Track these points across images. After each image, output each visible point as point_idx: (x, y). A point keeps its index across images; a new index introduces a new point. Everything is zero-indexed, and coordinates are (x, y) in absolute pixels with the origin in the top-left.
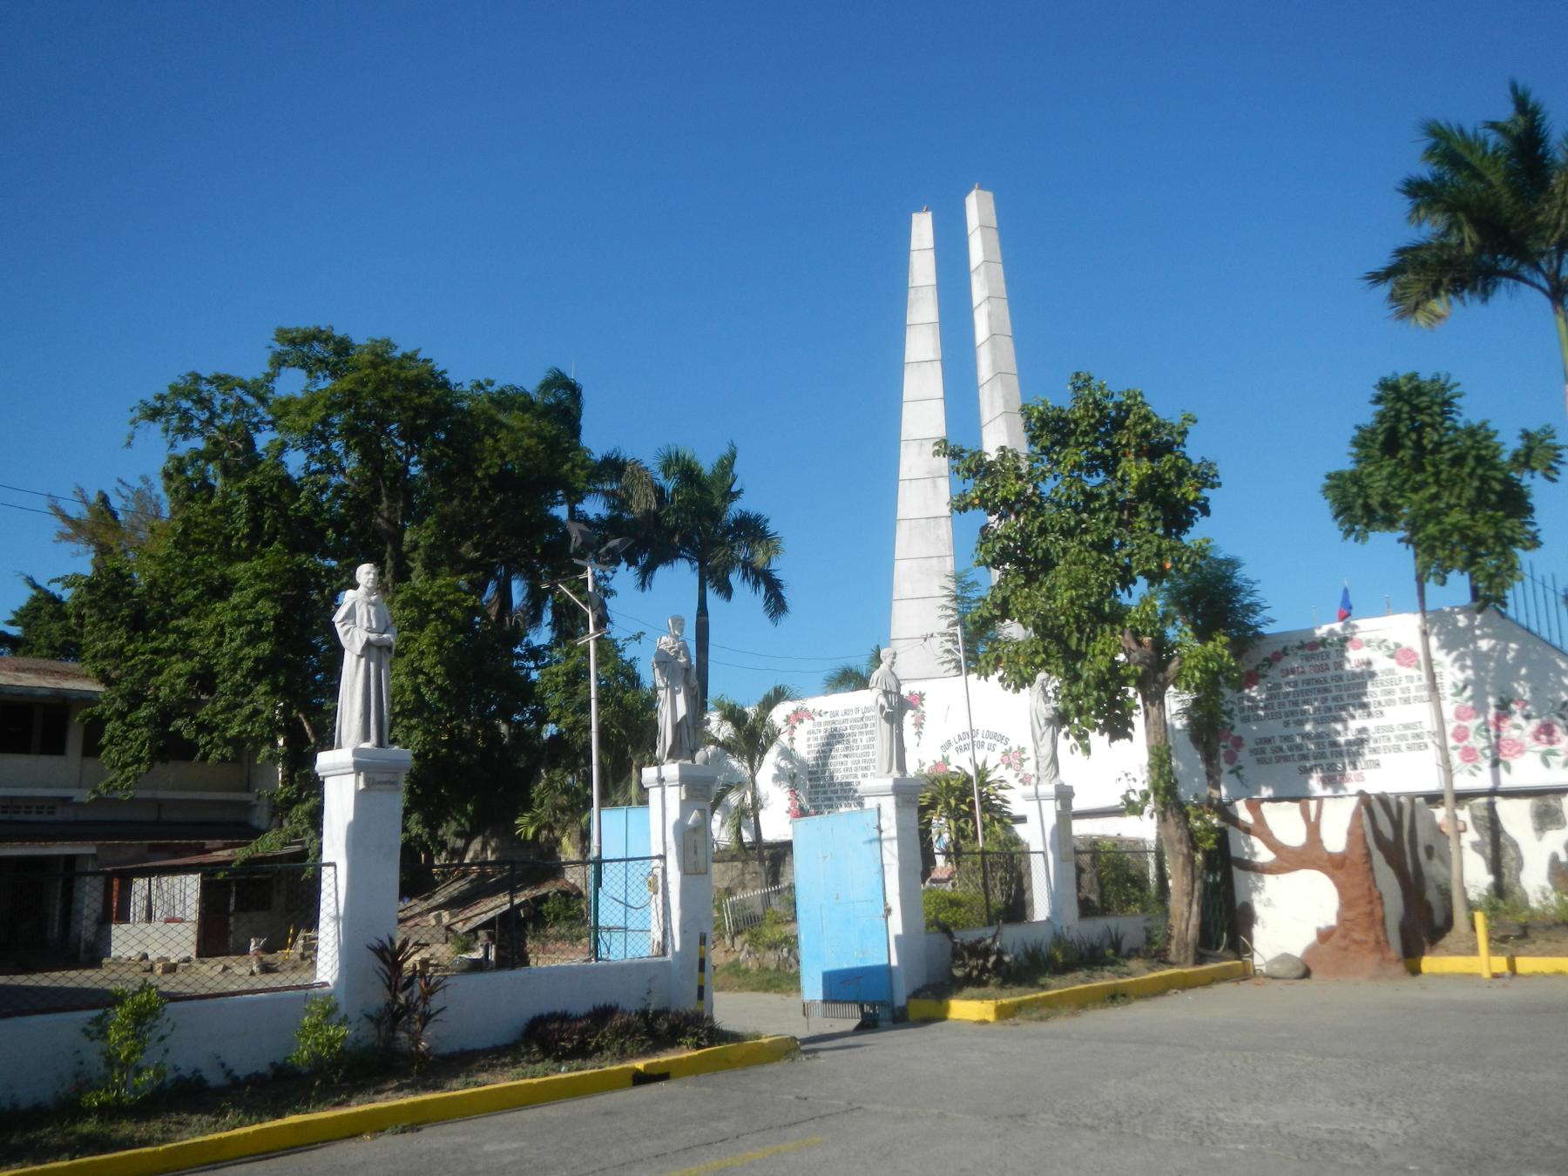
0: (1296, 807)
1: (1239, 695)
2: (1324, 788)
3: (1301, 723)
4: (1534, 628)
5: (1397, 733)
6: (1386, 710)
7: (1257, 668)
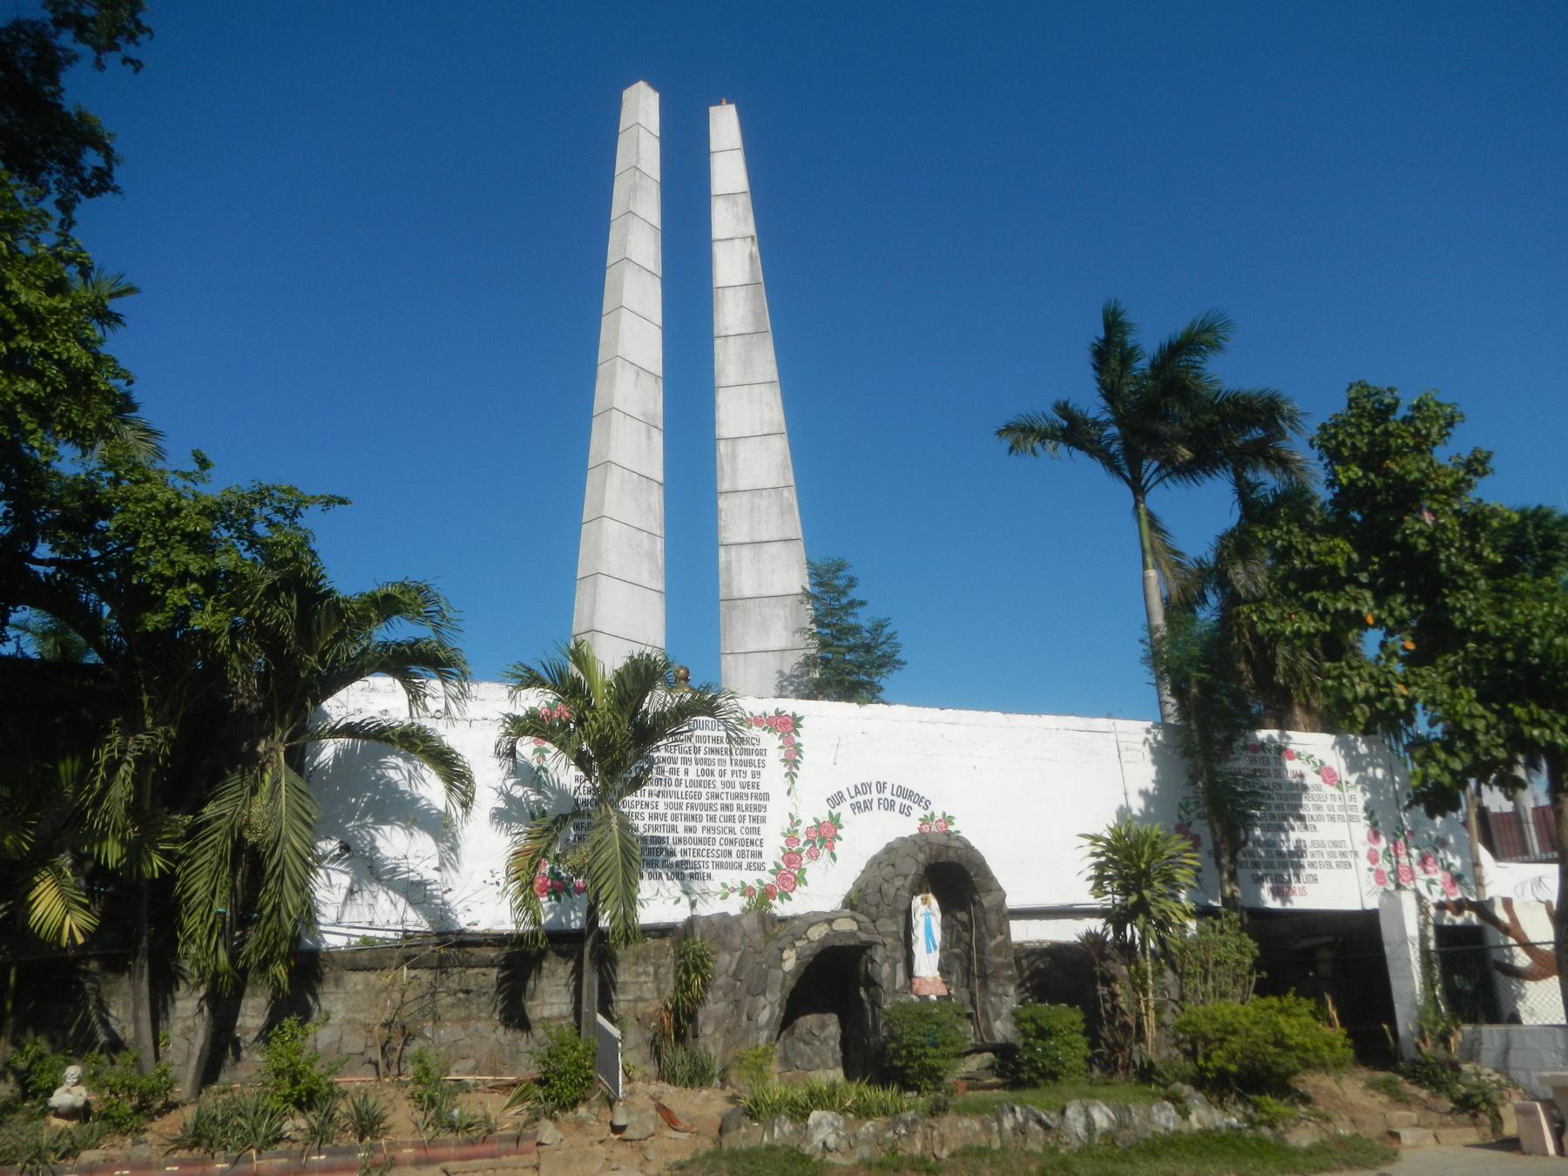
2: (1274, 899)
5: (1328, 849)
6: (1319, 825)
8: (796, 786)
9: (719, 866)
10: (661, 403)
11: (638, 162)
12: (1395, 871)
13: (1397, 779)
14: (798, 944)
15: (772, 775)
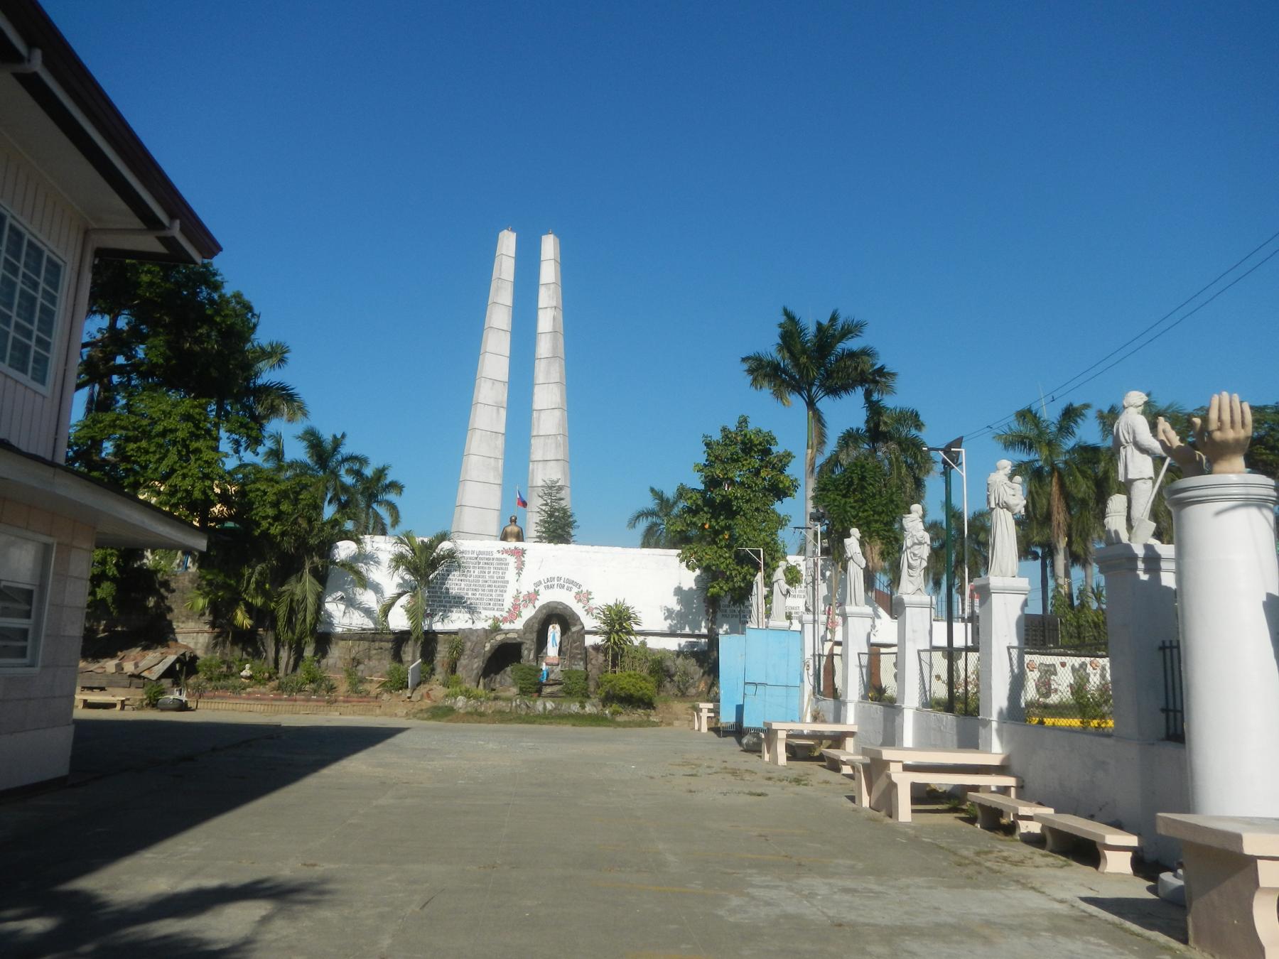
8: (520, 578)
9: (485, 609)
10: (506, 395)
11: (500, 275)
14: (492, 641)
15: (511, 574)
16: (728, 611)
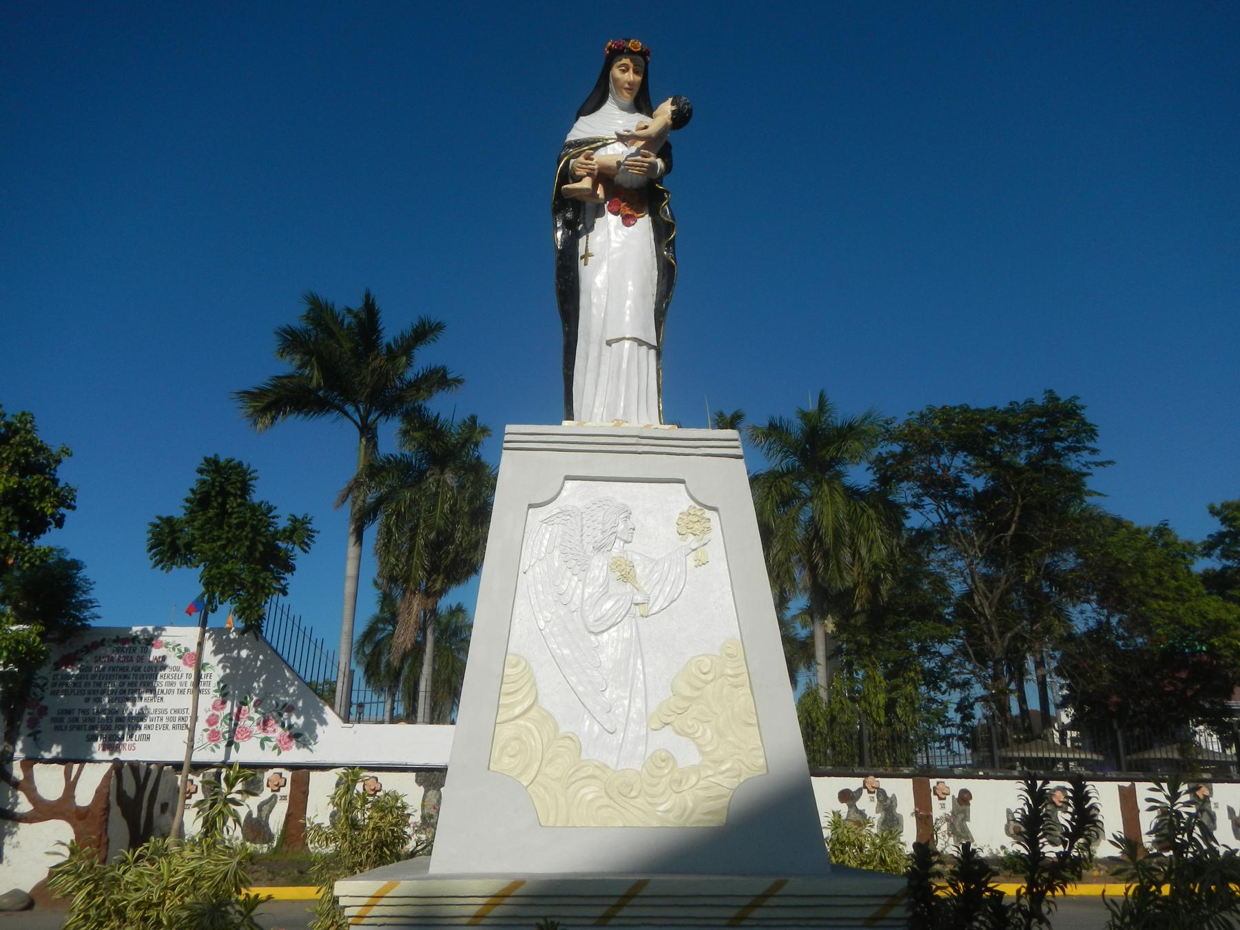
0: (63, 767)
1: (56, 673)
3: (99, 700)
4: (280, 650)
5: (169, 715)
6: (166, 697)
7: (77, 652)
12: (232, 732)
13: (261, 657)
16: (66, 719)
